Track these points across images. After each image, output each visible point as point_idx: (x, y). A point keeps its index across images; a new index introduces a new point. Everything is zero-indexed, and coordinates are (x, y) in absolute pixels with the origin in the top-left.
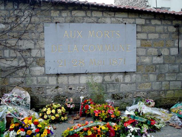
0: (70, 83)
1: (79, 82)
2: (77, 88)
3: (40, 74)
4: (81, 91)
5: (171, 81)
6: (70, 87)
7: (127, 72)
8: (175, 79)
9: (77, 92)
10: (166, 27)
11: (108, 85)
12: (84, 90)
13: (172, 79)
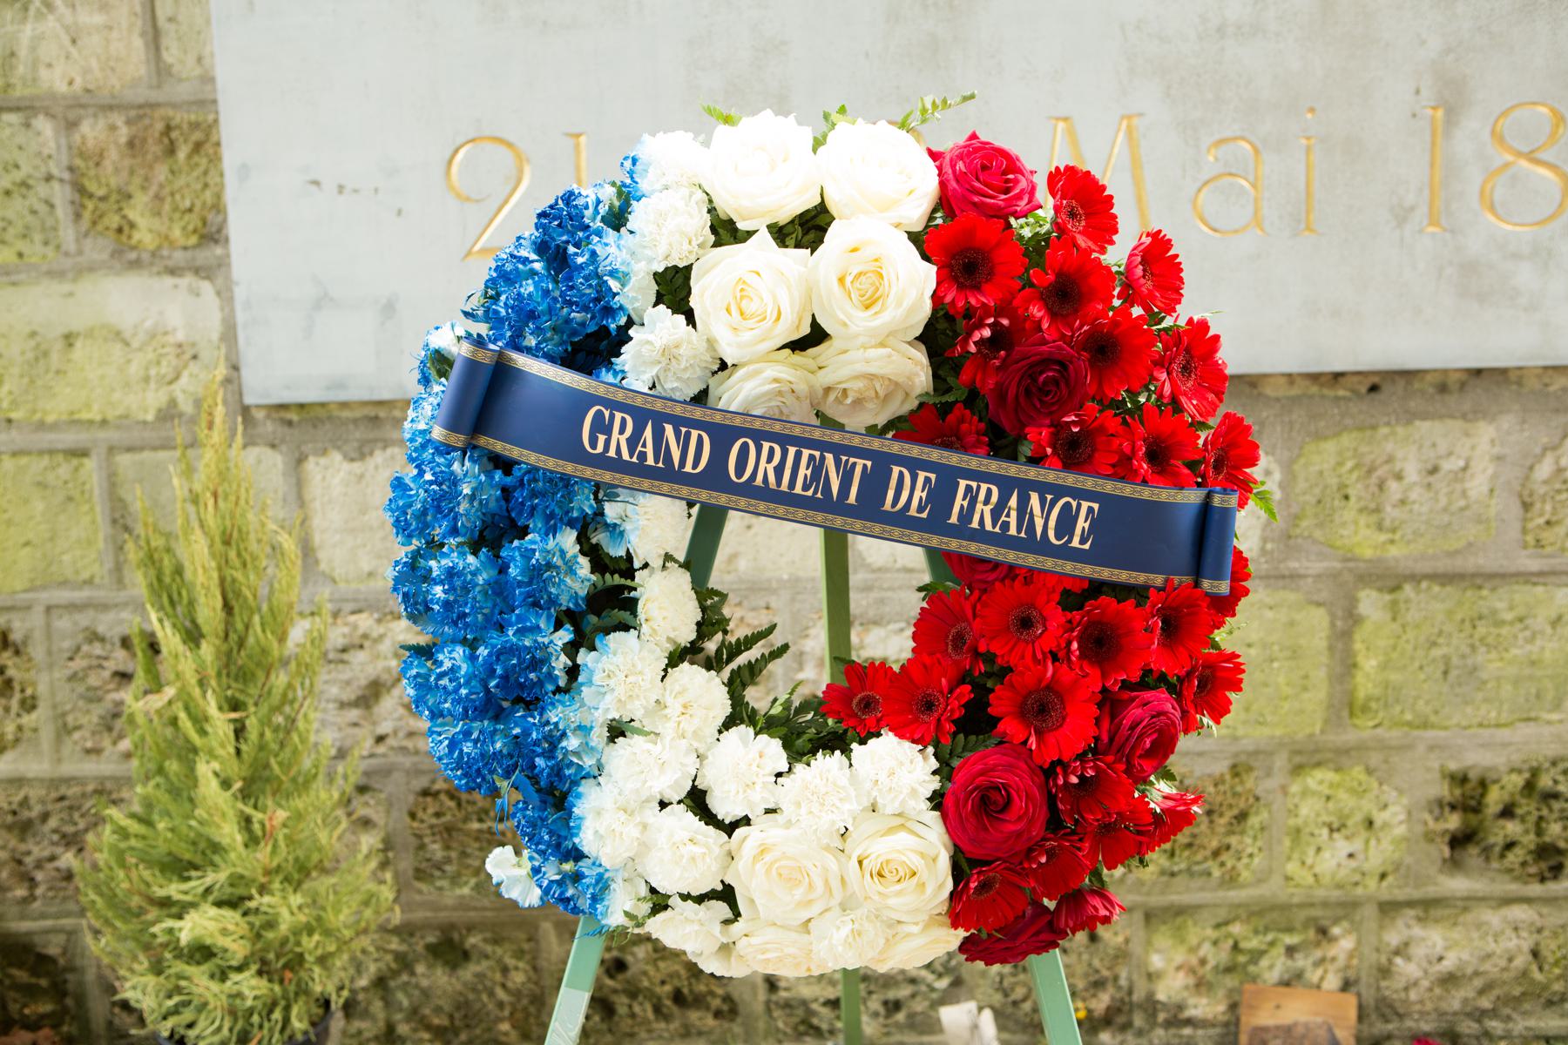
3: (149, 403)
11: (1370, 603)
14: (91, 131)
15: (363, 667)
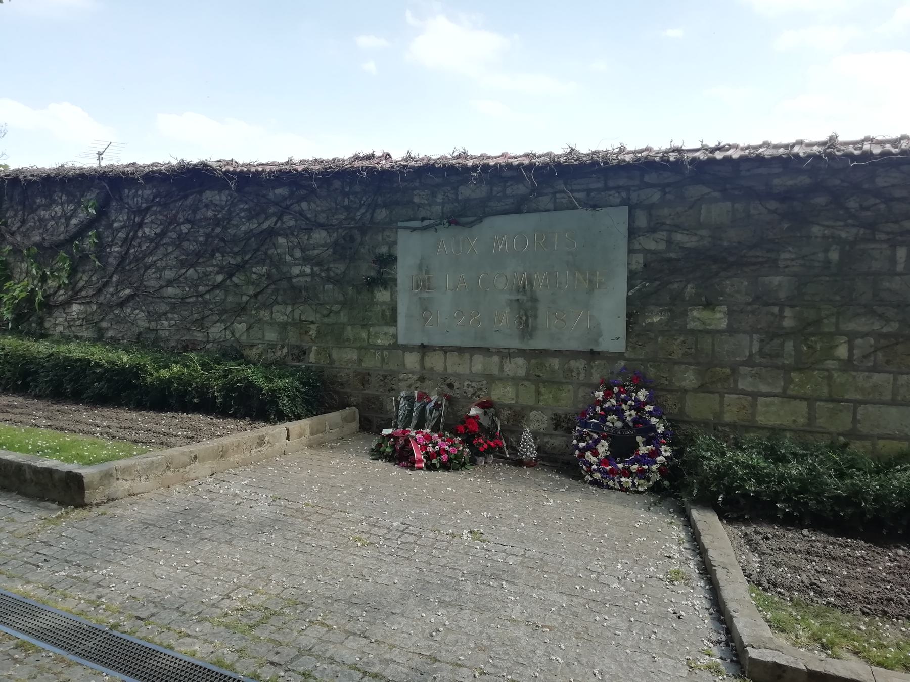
0: (450, 371)
1: (470, 370)
2: (466, 384)
4: (474, 394)
5: (761, 396)
6: (448, 381)
7: (599, 353)
8: (778, 390)
9: (465, 394)
10: (739, 206)
12: (479, 392)
13: (764, 388)
14: (384, 307)
15: (410, 382)
